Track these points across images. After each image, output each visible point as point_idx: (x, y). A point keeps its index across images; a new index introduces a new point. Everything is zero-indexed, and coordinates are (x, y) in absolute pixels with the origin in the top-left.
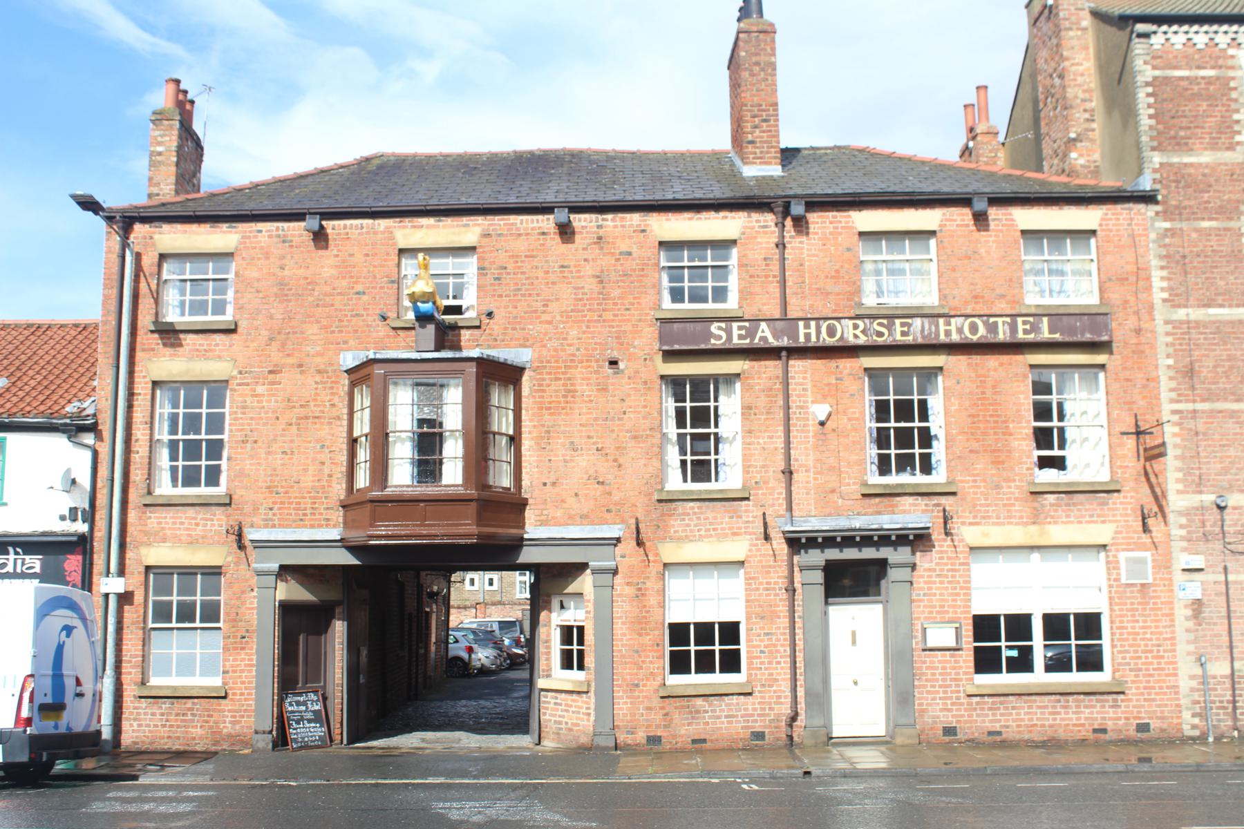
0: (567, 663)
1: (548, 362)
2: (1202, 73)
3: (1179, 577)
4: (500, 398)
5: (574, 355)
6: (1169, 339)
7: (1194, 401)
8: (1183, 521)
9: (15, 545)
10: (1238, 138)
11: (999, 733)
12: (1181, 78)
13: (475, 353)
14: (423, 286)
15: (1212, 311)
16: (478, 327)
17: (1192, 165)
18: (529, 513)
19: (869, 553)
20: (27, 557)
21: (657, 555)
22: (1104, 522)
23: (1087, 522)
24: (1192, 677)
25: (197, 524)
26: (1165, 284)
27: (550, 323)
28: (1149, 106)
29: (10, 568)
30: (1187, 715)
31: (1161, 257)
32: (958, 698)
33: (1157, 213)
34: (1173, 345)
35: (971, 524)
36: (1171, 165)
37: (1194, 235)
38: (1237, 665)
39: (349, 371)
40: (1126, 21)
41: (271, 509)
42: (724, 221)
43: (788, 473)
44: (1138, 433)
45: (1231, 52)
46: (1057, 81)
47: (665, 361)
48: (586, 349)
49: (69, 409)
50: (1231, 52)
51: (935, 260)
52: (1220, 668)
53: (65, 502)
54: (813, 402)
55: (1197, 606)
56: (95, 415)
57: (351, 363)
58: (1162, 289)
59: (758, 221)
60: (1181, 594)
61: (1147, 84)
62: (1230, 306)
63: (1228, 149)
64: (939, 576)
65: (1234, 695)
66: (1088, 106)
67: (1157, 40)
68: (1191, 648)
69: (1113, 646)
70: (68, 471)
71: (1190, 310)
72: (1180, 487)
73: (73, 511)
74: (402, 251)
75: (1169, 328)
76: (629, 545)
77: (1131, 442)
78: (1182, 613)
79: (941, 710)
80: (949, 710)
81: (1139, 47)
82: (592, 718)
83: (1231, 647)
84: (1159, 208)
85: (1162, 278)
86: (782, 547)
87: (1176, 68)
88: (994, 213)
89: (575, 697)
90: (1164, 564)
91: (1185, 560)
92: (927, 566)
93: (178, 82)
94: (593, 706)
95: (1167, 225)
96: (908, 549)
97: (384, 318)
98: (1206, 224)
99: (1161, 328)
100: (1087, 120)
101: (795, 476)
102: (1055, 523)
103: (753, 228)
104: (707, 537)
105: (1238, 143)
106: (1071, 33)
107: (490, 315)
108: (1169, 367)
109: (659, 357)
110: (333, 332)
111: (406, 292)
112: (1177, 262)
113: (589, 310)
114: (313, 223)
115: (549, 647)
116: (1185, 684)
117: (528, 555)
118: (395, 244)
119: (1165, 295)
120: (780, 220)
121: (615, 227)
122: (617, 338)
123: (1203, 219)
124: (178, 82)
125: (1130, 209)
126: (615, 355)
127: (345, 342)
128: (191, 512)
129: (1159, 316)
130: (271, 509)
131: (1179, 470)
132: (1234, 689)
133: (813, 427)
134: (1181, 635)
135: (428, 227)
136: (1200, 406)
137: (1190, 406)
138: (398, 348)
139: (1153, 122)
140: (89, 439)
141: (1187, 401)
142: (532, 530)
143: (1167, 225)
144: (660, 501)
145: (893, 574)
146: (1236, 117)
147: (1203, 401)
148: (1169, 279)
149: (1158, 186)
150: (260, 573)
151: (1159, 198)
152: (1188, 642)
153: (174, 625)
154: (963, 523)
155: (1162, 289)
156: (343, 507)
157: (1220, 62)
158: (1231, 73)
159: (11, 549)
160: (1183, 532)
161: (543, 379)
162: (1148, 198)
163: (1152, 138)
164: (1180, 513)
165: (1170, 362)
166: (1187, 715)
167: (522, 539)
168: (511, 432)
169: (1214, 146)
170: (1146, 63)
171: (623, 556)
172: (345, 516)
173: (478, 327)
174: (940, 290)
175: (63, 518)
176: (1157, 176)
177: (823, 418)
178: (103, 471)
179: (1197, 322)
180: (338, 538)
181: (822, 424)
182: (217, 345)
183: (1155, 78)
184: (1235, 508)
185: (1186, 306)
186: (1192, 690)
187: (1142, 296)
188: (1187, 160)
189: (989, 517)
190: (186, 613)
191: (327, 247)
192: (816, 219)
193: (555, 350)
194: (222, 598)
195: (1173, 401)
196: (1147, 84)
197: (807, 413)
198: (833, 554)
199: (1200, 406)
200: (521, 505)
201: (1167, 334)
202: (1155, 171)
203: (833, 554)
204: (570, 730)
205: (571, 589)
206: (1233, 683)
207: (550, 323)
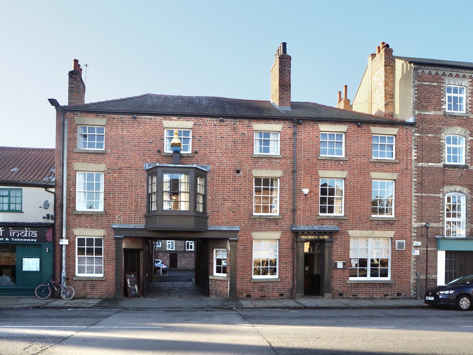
2: (433, 84)
3: (413, 248)
4: (200, 181)
5: (225, 168)
6: (416, 172)
7: (422, 193)
8: (416, 231)
9: (27, 227)
10: (442, 107)
11: (356, 295)
12: (426, 85)
15: (430, 164)
17: (427, 115)
18: (209, 221)
20: (32, 232)
22: (392, 230)
24: (414, 279)
25: (93, 222)
26: (416, 154)
27: (217, 156)
29: (26, 235)
30: (412, 291)
31: (416, 145)
33: (415, 131)
34: (417, 174)
35: (351, 229)
36: (421, 114)
37: (426, 139)
38: (428, 276)
39: (147, 170)
42: (277, 125)
45: (442, 77)
50: (442, 77)
52: (423, 277)
53: (45, 213)
54: (303, 188)
55: (417, 257)
58: (415, 156)
59: (288, 125)
60: (413, 254)
62: (435, 163)
63: (439, 110)
64: (340, 246)
65: (426, 285)
68: (415, 270)
69: (392, 269)
70: (47, 201)
71: (423, 163)
72: (415, 220)
73: (48, 215)
78: (413, 259)
80: (341, 288)
83: (427, 270)
84: (416, 129)
87: (425, 81)
90: (409, 245)
91: (416, 243)
92: (337, 242)
95: (418, 135)
98: (430, 135)
99: (414, 169)
102: (377, 230)
104: (267, 231)
105: (442, 109)
108: (415, 181)
110: (141, 156)
112: (420, 147)
113: (230, 153)
116: (412, 281)
118: (163, 126)
119: (416, 158)
122: (240, 163)
123: (429, 133)
125: (407, 128)
126: (238, 168)
127: (146, 160)
131: (416, 215)
132: (426, 283)
134: (412, 266)
135: (175, 120)
136: (423, 195)
137: (420, 194)
140: (53, 190)
141: (420, 193)
143: (418, 135)
146: (442, 100)
147: (425, 193)
148: (417, 153)
149: (417, 121)
152: (414, 269)
154: (349, 229)
155: (415, 156)
157: (439, 81)
158: (442, 85)
159: (26, 228)
160: (415, 234)
164: (415, 228)
165: (416, 180)
166: (412, 291)
168: (203, 193)
169: (435, 109)
171: (240, 236)
175: (44, 218)
176: (417, 118)
179: (425, 167)
181: (306, 195)
182: (99, 159)
183: (418, 84)
184: (431, 227)
185: (422, 162)
186: (414, 283)
187: (409, 158)
188: (426, 113)
189: (357, 228)
194: (103, 247)
195: (415, 193)
197: (301, 191)
199: (423, 195)
200: (207, 218)
201: (415, 171)
204: (221, 292)
206: (426, 281)
207: (217, 156)
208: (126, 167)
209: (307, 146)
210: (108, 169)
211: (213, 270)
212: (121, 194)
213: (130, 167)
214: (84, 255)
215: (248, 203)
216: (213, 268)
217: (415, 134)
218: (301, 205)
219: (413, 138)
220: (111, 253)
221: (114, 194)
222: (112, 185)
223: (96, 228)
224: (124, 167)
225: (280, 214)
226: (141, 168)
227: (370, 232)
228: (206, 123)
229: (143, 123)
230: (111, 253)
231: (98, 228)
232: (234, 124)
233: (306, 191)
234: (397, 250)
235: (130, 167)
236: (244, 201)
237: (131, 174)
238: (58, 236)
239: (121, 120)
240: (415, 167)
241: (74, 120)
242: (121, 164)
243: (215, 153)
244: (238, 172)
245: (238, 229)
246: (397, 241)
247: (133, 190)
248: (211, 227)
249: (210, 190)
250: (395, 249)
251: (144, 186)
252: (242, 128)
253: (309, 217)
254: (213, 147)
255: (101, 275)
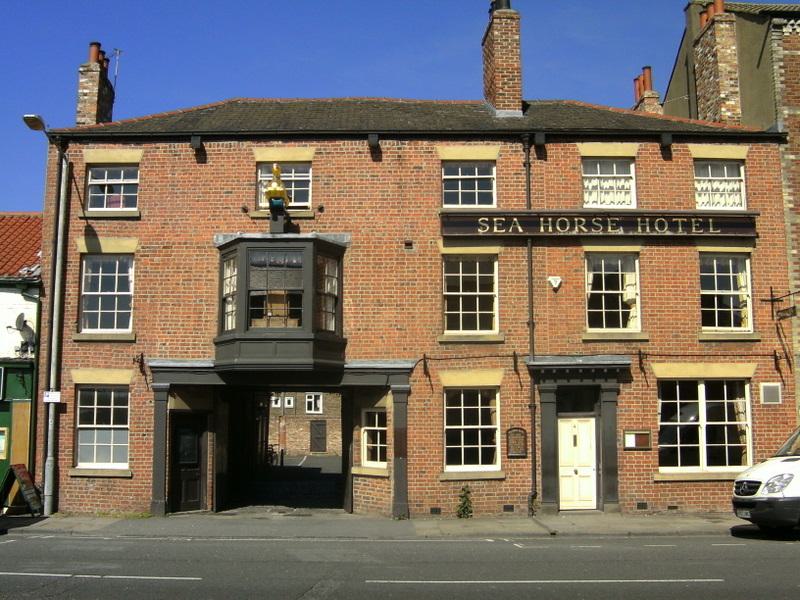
0: (372, 456)
1: (363, 243)
5: (381, 239)
11: (675, 508)
13: (309, 235)
14: (275, 186)
16: (313, 218)
18: (349, 349)
19: (588, 382)
21: (438, 380)
23: (738, 362)
26: (791, 198)
27: (364, 215)
28: (781, 75)
31: (789, 179)
32: (648, 483)
33: (786, 149)
34: (796, 240)
39: (221, 248)
40: (765, 16)
41: (164, 344)
43: (531, 324)
44: (773, 301)
46: (711, 59)
47: (445, 245)
48: (390, 235)
49: (23, 271)
51: (634, 177)
54: (550, 275)
56: (39, 276)
57: (221, 241)
58: (790, 202)
61: (781, 60)
66: (733, 76)
67: (787, 30)
69: (754, 448)
70: (22, 315)
74: (259, 164)
75: (794, 228)
76: (418, 373)
77: (768, 307)
79: (636, 492)
81: (775, 35)
82: (392, 495)
84: (788, 146)
85: (790, 194)
86: (526, 377)
88: (674, 146)
89: (379, 480)
92: (627, 391)
93: (99, 45)
94: (392, 486)
95: (792, 157)
96: (615, 380)
97: (245, 210)
100: (732, 86)
101: (537, 326)
103: (507, 152)
106: (722, 26)
107: (321, 209)
108: (794, 255)
109: (440, 242)
111: (264, 190)
113: (392, 207)
114: (197, 141)
115: (359, 445)
117: (348, 381)
118: (253, 158)
119: (791, 206)
120: (527, 146)
121: (410, 149)
124: (99, 45)
126: (409, 238)
128: (107, 346)
129: (788, 221)
130: (164, 344)
133: (549, 293)
135: (277, 146)
138: (254, 231)
139: (783, 86)
142: (351, 362)
143: (792, 157)
144: (441, 343)
145: (605, 396)
148: (794, 195)
150: (156, 390)
151: (788, 138)
153: (111, 426)
154: (653, 361)
155: (790, 202)
156: (216, 344)
161: (359, 255)
162: (780, 139)
163: (783, 98)
165: (795, 252)
167: (342, 368)
170: (779, 45)
172: (217, 353)
173: (313, 218)
174: (637, 199)
176: (787, 123)
177: (556, 285)
178: (45, 316)
180: (212, 365)
181: (556, 290)
183: (785, 56)
190: (104, 417)
191: (205, 162)
192: (552, 149)
193: (367, 235)
194: (129, 407)
196: (781, 60)
198: (564, 382)
200: (343, 343)
201: (793, 232)
202: (785, 120)
203: (564, 382)
205: (376, 405)
207: (364, 215)
208: (180, 243)
209: (553, 187)
210: (143, 248)
211: (359, 454)
212: (168, 297)
213: (185, 243)
214: (109, 423)
215: (431, 309)
216: (359, 449)
217: (786, 157)
218: (543, 312)
219: (783, 164)
220: (144, 419)
221: (153, 297)
222: (151, 280)
223: (115, 368)
224: (174, 243)
225: (500, 331)
226: (208, 243)
227: (701, 366)
228: (341, 149)
229: (216, 154)
230: (144, 419)
231: (120, 368)
232: (399, 149)
233: (555, 281)
234: (764, 406)
235: (185, 243)
236: (421, 305)
237: (187, 256)
238: (42, 383)
239: (171, 151)
240: (793, 225)
241: (82, 156)
242: (169, 238)
243: (359, 208)
244: (409, 245)
245: (410, 366)
246: (762, 385)
247: (191, 289)
248: (351, 362)
249: (350, 284)
250: (758, 402)
251: (213, 280)
252: (416, 156)
253: (563, 337)
254: (356, 196)
255: (125, 466)
